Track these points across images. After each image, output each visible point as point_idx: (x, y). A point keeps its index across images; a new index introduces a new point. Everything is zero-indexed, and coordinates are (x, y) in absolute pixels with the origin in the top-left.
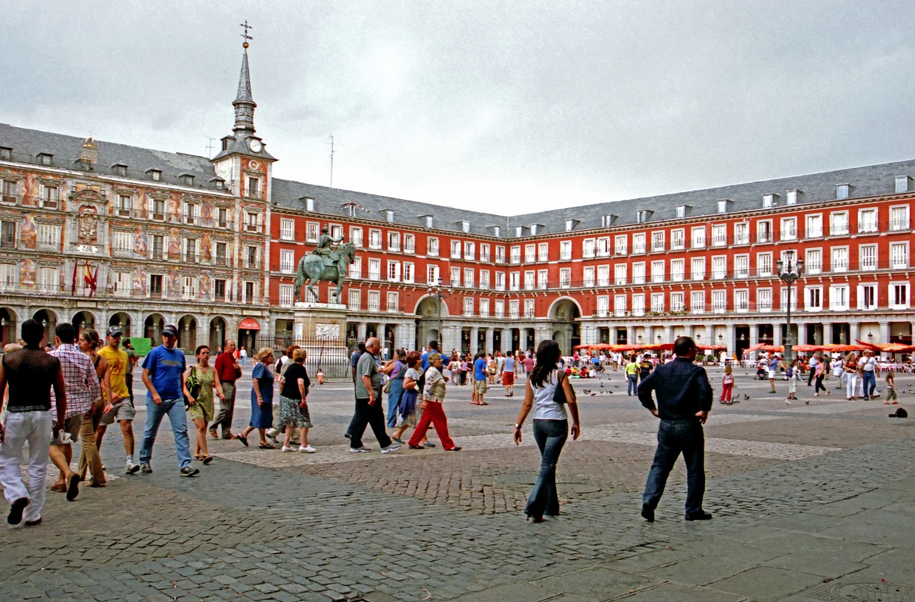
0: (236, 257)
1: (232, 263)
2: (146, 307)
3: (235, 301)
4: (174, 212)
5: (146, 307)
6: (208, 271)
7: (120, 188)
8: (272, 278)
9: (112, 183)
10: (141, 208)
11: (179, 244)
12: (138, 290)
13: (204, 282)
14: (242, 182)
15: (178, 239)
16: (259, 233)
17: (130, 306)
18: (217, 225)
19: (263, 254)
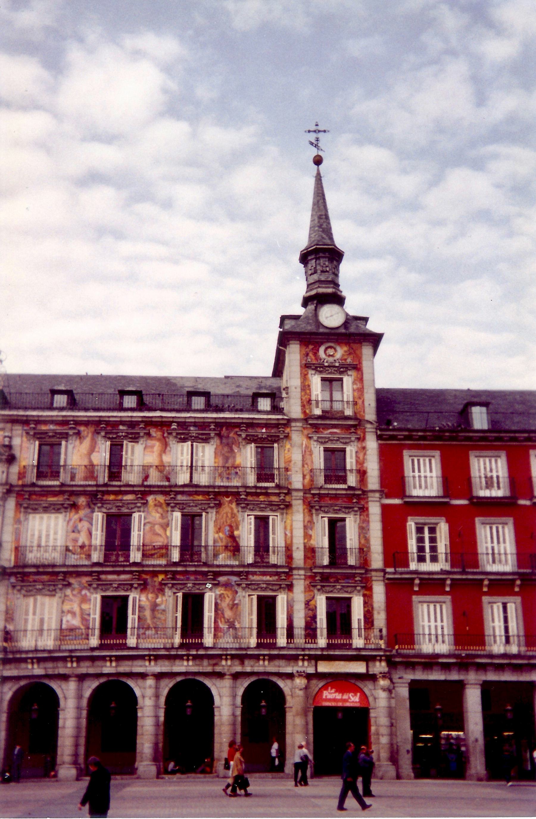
0: (299, 542)
1: (289, 557)
2: (85, 668)
3: (299, 640)
4: (156, 462)
5: (85, 668)
6: (234, 579)
7: (44, 428)
8: (392, 586)
9: (25, 422)
10: (86, 462)
11: (166, 526)
12: (72, 630)
13: (225, 604)
14: (306, 388)
15: (162, 517)
16: (350, 488)
17: (51, 668)
18: (251, 480)
19: (363, 530)
